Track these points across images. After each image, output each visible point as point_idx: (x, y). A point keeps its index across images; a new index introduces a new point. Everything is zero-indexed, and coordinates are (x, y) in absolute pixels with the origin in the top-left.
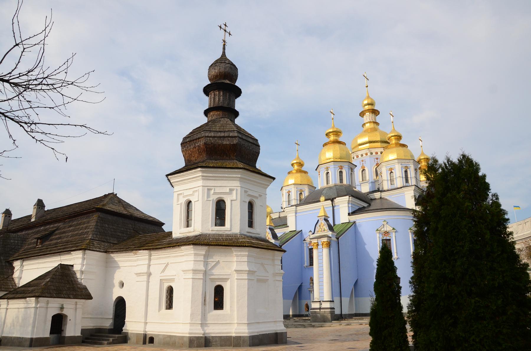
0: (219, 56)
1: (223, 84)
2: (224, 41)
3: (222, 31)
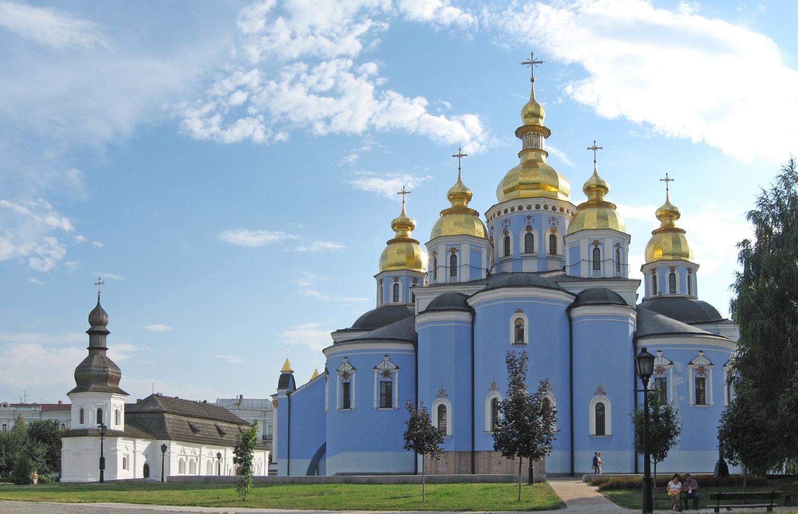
1: (98, 328)
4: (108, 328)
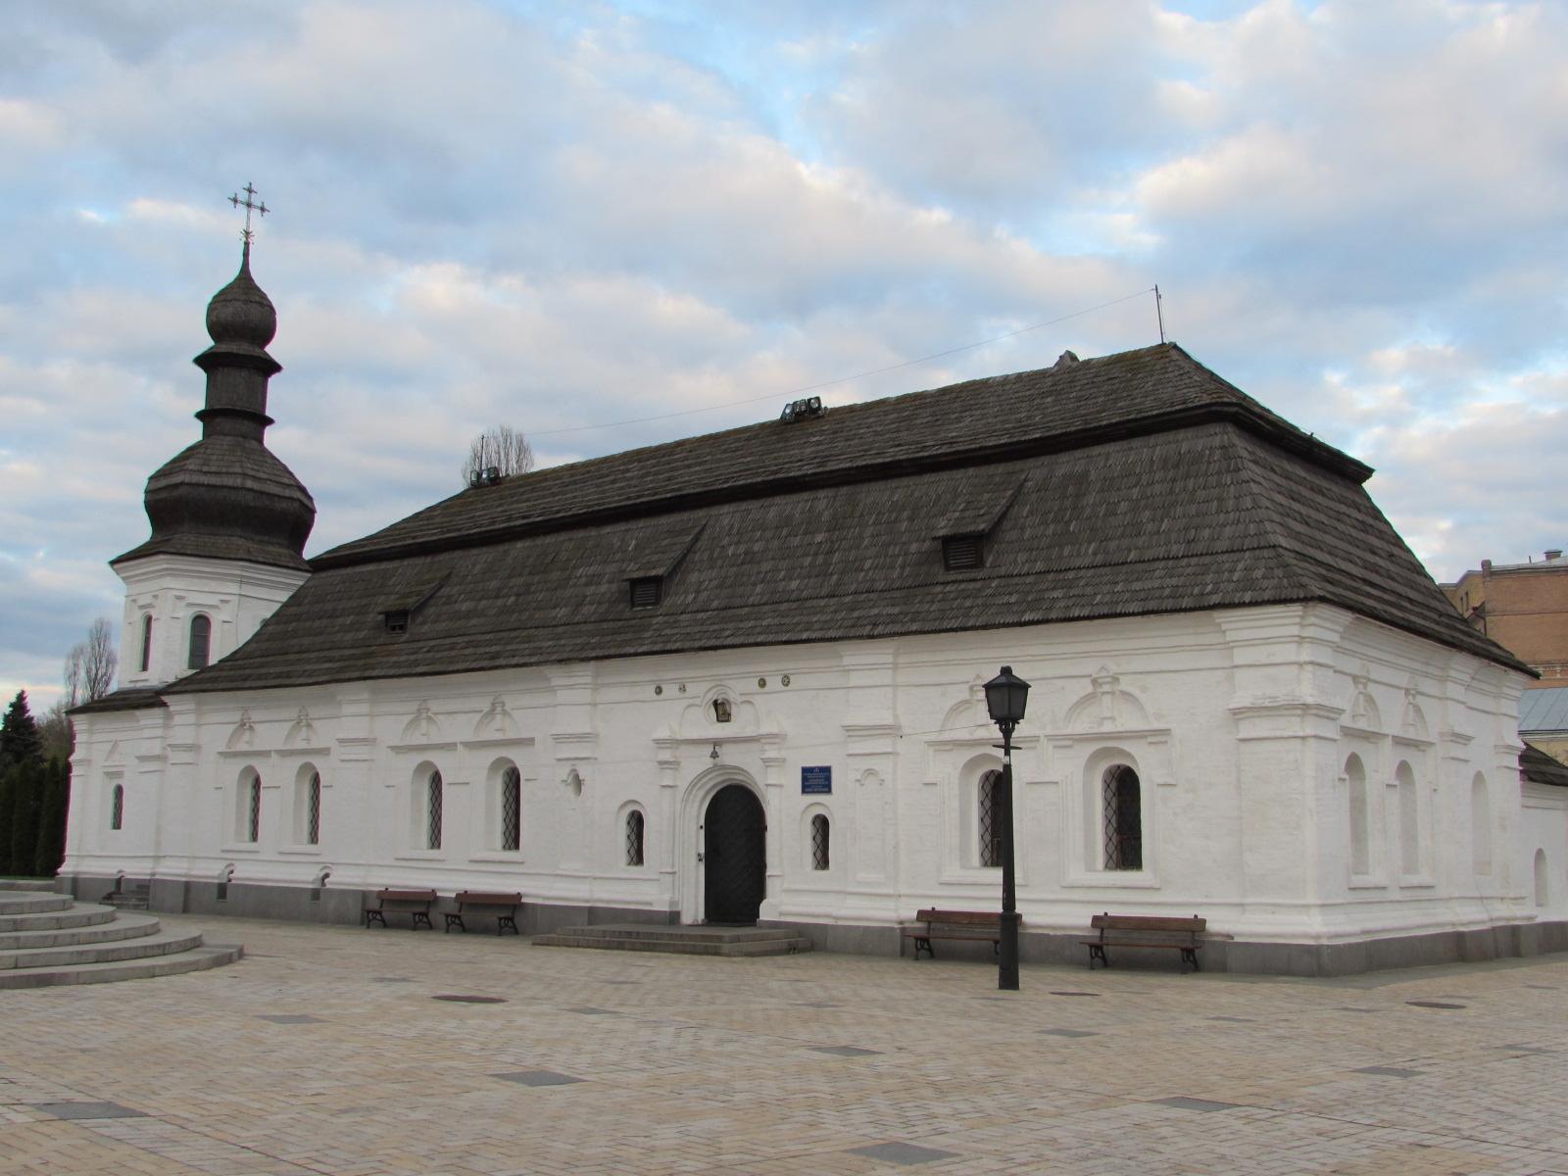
0: (231, 274)
1: (240, 343)
2: (247, 234)
3: (242, 209)
4: (273, 350)
